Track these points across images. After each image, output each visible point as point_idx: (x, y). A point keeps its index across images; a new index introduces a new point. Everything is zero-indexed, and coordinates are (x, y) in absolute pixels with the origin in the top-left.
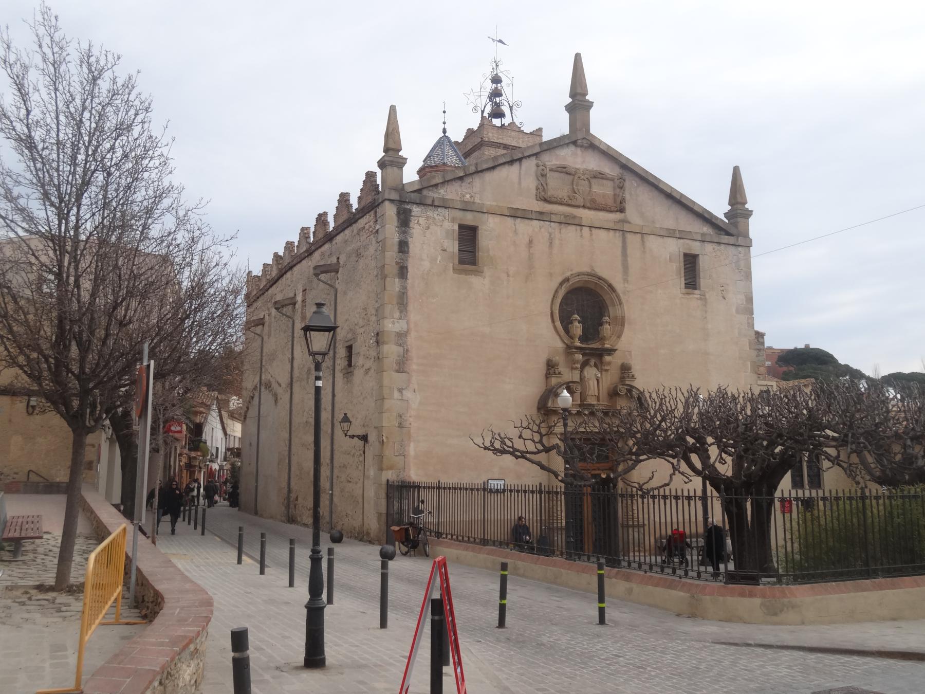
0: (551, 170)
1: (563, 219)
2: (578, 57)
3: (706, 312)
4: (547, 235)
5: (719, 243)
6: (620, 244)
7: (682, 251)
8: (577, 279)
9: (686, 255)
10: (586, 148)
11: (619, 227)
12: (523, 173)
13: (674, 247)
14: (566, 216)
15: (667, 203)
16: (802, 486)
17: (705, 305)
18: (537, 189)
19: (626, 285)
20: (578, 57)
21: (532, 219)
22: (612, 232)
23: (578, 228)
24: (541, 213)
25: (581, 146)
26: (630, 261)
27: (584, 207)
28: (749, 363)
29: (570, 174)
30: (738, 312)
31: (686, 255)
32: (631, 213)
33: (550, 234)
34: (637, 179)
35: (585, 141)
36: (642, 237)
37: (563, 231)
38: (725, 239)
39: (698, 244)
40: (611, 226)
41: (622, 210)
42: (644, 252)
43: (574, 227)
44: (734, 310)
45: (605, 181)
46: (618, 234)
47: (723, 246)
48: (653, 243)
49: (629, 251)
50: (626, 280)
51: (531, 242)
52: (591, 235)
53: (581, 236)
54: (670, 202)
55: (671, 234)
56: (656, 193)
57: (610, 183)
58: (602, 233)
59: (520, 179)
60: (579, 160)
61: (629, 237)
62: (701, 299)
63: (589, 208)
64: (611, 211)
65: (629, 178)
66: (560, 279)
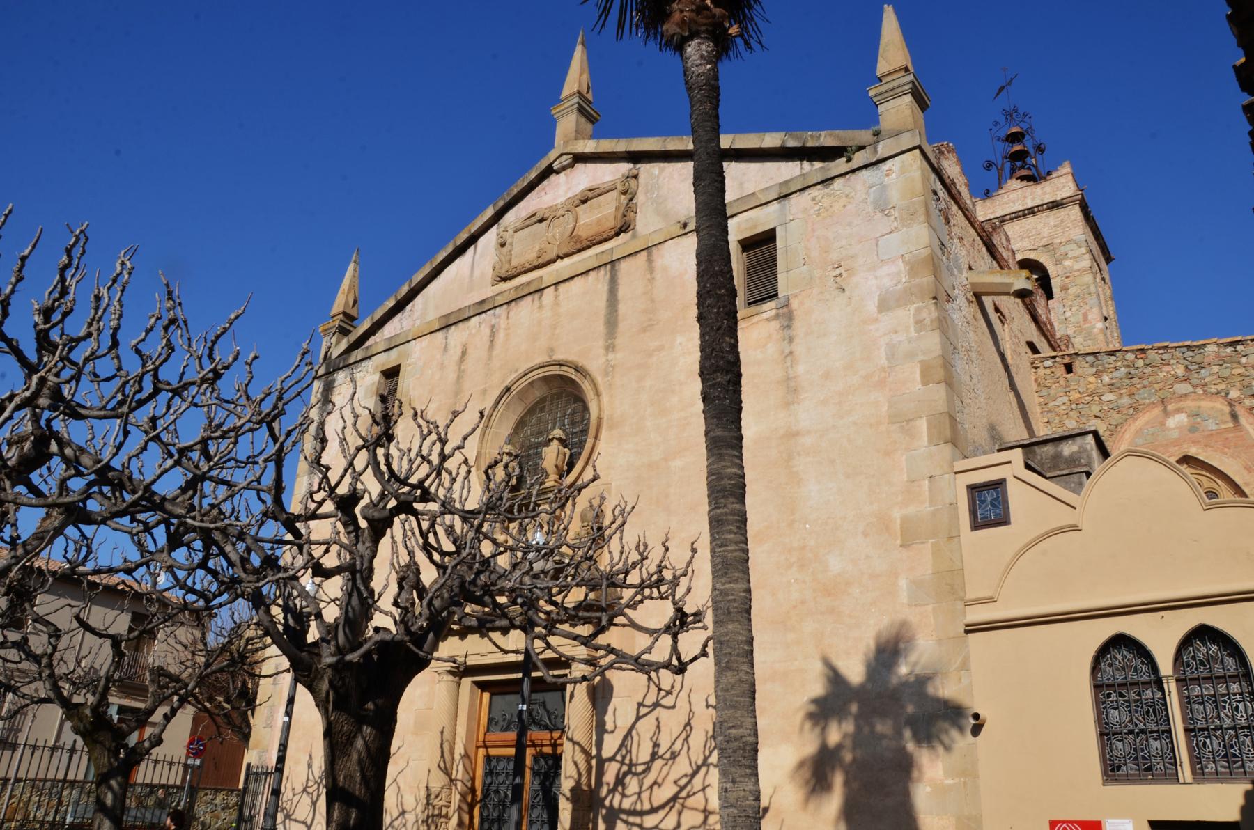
3: (791, 340)
4: (488, 331)
5: (826, 181)
6: (606, 288)
8: (525, 382)
10: (571, 165)
14: (516, 288)
16: (1154, 768)
17: (789, 327)
19: (611, 356)
21: (469, 318)
23: (537, 296)
24: (482, 302)
25: (564, 168)
26: (622, 308)
27: (562, 258)
28: (922, 425)
30: (884, 306)
33: (493, 327)
37: (512, 313)
38: (840, 165)
39: (775, 206)
41: (624, 228)
42: (651, 280)
43: (529, 298)
44: (872, 306)
46: (602, 271)
47: (838, 183)
49: (622, 292)
50: (610, 348)
51: (464, 353)
52: (556, 297)
53: (540, 307)
57: (614, 193)
62: (777, 317)
63: (568, 255)
65: (646, 169)
66: (497, 393)
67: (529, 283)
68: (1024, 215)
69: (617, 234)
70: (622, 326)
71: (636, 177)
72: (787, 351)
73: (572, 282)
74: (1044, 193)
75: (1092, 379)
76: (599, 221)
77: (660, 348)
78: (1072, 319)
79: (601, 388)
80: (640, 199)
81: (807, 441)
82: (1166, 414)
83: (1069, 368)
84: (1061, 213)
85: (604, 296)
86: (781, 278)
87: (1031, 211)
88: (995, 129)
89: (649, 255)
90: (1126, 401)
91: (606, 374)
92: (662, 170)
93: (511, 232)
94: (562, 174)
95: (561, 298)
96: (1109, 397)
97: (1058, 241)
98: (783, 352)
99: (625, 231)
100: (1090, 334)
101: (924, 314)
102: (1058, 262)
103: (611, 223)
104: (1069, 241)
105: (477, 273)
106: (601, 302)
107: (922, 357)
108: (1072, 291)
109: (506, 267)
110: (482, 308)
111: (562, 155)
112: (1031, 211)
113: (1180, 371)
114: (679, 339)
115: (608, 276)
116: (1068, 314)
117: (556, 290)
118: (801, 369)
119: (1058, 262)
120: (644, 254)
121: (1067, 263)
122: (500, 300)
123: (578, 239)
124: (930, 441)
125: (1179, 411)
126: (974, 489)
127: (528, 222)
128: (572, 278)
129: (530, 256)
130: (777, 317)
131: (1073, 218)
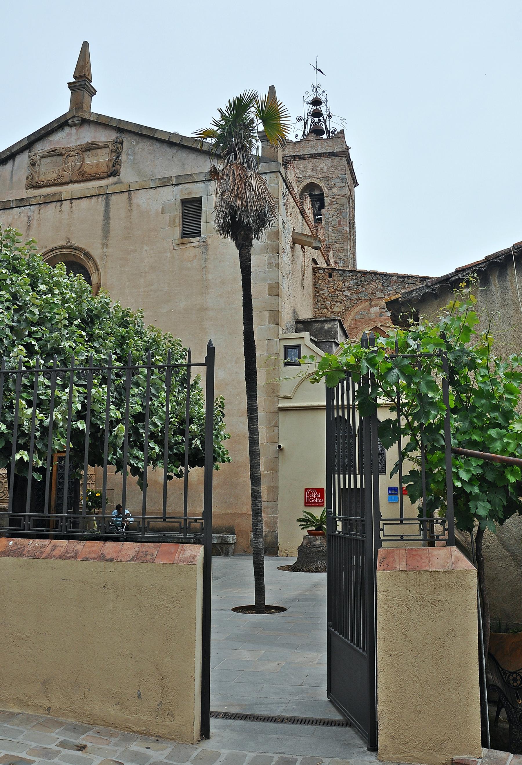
0: (42, 157)
1: (42, 200)
2: (85, 45)
3: (206, 260)
4: (26, 219)
6: (103, 209)
7: (179, 197)
9: (185, 202)
11: (103, 191)
12: (15, 168)
13: (172, 196)
14: (45, 196)
15: (169, 151)
17: (206, 253)
18: (27, 178)
19: (105, 250)
20: (85, 45)
21: (12, 208)
22: (94, 199)
23: (58, 204)
24: (21, 200)
25: (75, 125)
26: (112, 223)
27: (71, 182)
29: (61, 155)
31: (185, 202)
32: (128, 175)
34: (135, 138)
35: (76, 119)
36: (130, 195)
39: (202, 185)
40: (94, 192)
41: (114, 173)
42: (130, 210)
43: (54, 204)
45: (99, 151)
46: (100, 198)
48: (142, 199)
49: (112, 213)
50: (105, 245)
53: (60, 211)
54: (174, 150)
55: (165, 183)
56: (157, 145)
57: (107, 151)
58: (84, 203)
59: (12, 175)
60: (73, 139)
61: (113, 198)
64: (103, 178)
67: (54, 195)
68: (316, 157)
69: (109, 176)
70: (112, 233)
71: (121, 143)
72: (204, 266)
73: (81, 200)
74: (328, 146)
75: (340, 283)
76: (97, 165)
77: (135, 251)
78: (333, 223)
79: (100, 267)
80: (123, 157)
81: (211, 313)
82: (371, 306)
83: (330, 276)
84: (336, 160)
85: (102, 214)
86: (203, 226)
87: (320, 156)
88: (306, 96)
89: (130, 195)
90: (354, 296)
91: (102, 259)
92: (138, 143)
93: (39, 157)
94: (73, 128)
95: (74, 208)
96: (347, 293)
97: (331, 176)
98: (201, 266)
99: (114, 175)
100: (341, 232)
101: (273, 261)
102: (330, 188)
103: (104, 169)
104: (337, 178)
105: (15, 178)
106: (100, 217)
107: (269, 282)
108: (334, 206)
109: (36, 180)
110: (21, 203)
111: (74, 117)
112: (320, 156)
113: (380, 286)
114: (145, 248)
115: (104, 202)
116: (331, 219)
117: (71, 203)
118: (210, 276)
119: (330, 188)
120: (127, 193)
121: (334, 190)
122: (33, 201)
123: (81, 172)
124: (269, 322)
125: (376, 305)
126: (286, 348)
127: (50, 154)
128: (81, 198)
129: (52, 176)
130: (200, 246)
131: (341, 164)
